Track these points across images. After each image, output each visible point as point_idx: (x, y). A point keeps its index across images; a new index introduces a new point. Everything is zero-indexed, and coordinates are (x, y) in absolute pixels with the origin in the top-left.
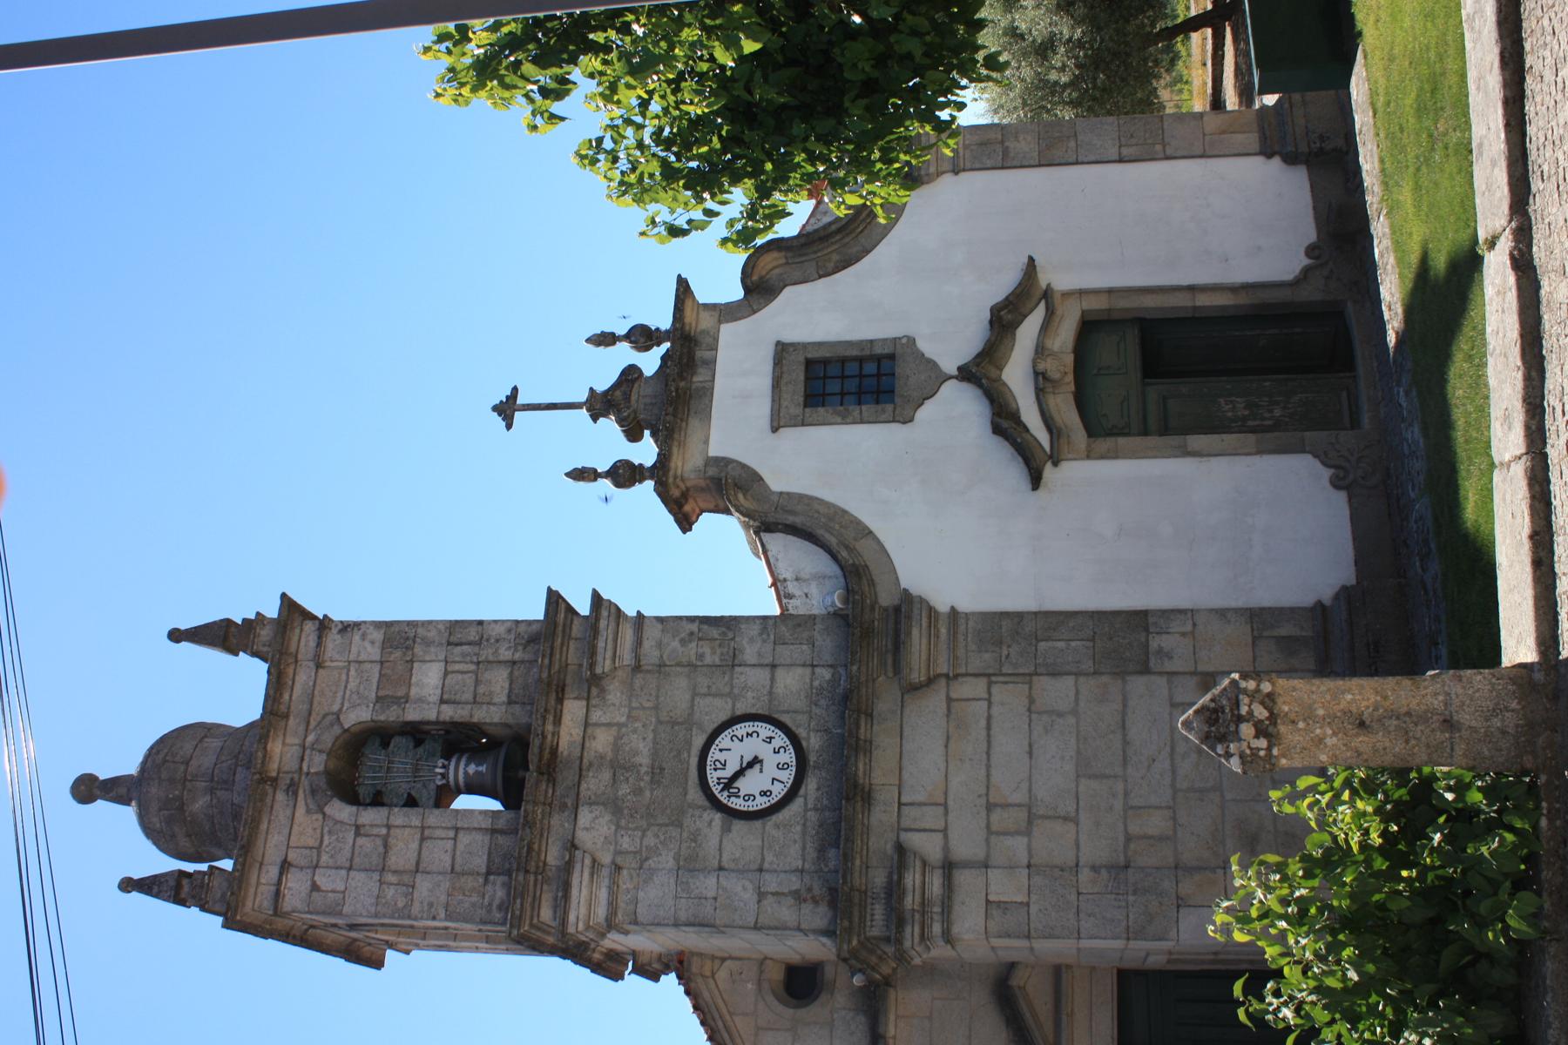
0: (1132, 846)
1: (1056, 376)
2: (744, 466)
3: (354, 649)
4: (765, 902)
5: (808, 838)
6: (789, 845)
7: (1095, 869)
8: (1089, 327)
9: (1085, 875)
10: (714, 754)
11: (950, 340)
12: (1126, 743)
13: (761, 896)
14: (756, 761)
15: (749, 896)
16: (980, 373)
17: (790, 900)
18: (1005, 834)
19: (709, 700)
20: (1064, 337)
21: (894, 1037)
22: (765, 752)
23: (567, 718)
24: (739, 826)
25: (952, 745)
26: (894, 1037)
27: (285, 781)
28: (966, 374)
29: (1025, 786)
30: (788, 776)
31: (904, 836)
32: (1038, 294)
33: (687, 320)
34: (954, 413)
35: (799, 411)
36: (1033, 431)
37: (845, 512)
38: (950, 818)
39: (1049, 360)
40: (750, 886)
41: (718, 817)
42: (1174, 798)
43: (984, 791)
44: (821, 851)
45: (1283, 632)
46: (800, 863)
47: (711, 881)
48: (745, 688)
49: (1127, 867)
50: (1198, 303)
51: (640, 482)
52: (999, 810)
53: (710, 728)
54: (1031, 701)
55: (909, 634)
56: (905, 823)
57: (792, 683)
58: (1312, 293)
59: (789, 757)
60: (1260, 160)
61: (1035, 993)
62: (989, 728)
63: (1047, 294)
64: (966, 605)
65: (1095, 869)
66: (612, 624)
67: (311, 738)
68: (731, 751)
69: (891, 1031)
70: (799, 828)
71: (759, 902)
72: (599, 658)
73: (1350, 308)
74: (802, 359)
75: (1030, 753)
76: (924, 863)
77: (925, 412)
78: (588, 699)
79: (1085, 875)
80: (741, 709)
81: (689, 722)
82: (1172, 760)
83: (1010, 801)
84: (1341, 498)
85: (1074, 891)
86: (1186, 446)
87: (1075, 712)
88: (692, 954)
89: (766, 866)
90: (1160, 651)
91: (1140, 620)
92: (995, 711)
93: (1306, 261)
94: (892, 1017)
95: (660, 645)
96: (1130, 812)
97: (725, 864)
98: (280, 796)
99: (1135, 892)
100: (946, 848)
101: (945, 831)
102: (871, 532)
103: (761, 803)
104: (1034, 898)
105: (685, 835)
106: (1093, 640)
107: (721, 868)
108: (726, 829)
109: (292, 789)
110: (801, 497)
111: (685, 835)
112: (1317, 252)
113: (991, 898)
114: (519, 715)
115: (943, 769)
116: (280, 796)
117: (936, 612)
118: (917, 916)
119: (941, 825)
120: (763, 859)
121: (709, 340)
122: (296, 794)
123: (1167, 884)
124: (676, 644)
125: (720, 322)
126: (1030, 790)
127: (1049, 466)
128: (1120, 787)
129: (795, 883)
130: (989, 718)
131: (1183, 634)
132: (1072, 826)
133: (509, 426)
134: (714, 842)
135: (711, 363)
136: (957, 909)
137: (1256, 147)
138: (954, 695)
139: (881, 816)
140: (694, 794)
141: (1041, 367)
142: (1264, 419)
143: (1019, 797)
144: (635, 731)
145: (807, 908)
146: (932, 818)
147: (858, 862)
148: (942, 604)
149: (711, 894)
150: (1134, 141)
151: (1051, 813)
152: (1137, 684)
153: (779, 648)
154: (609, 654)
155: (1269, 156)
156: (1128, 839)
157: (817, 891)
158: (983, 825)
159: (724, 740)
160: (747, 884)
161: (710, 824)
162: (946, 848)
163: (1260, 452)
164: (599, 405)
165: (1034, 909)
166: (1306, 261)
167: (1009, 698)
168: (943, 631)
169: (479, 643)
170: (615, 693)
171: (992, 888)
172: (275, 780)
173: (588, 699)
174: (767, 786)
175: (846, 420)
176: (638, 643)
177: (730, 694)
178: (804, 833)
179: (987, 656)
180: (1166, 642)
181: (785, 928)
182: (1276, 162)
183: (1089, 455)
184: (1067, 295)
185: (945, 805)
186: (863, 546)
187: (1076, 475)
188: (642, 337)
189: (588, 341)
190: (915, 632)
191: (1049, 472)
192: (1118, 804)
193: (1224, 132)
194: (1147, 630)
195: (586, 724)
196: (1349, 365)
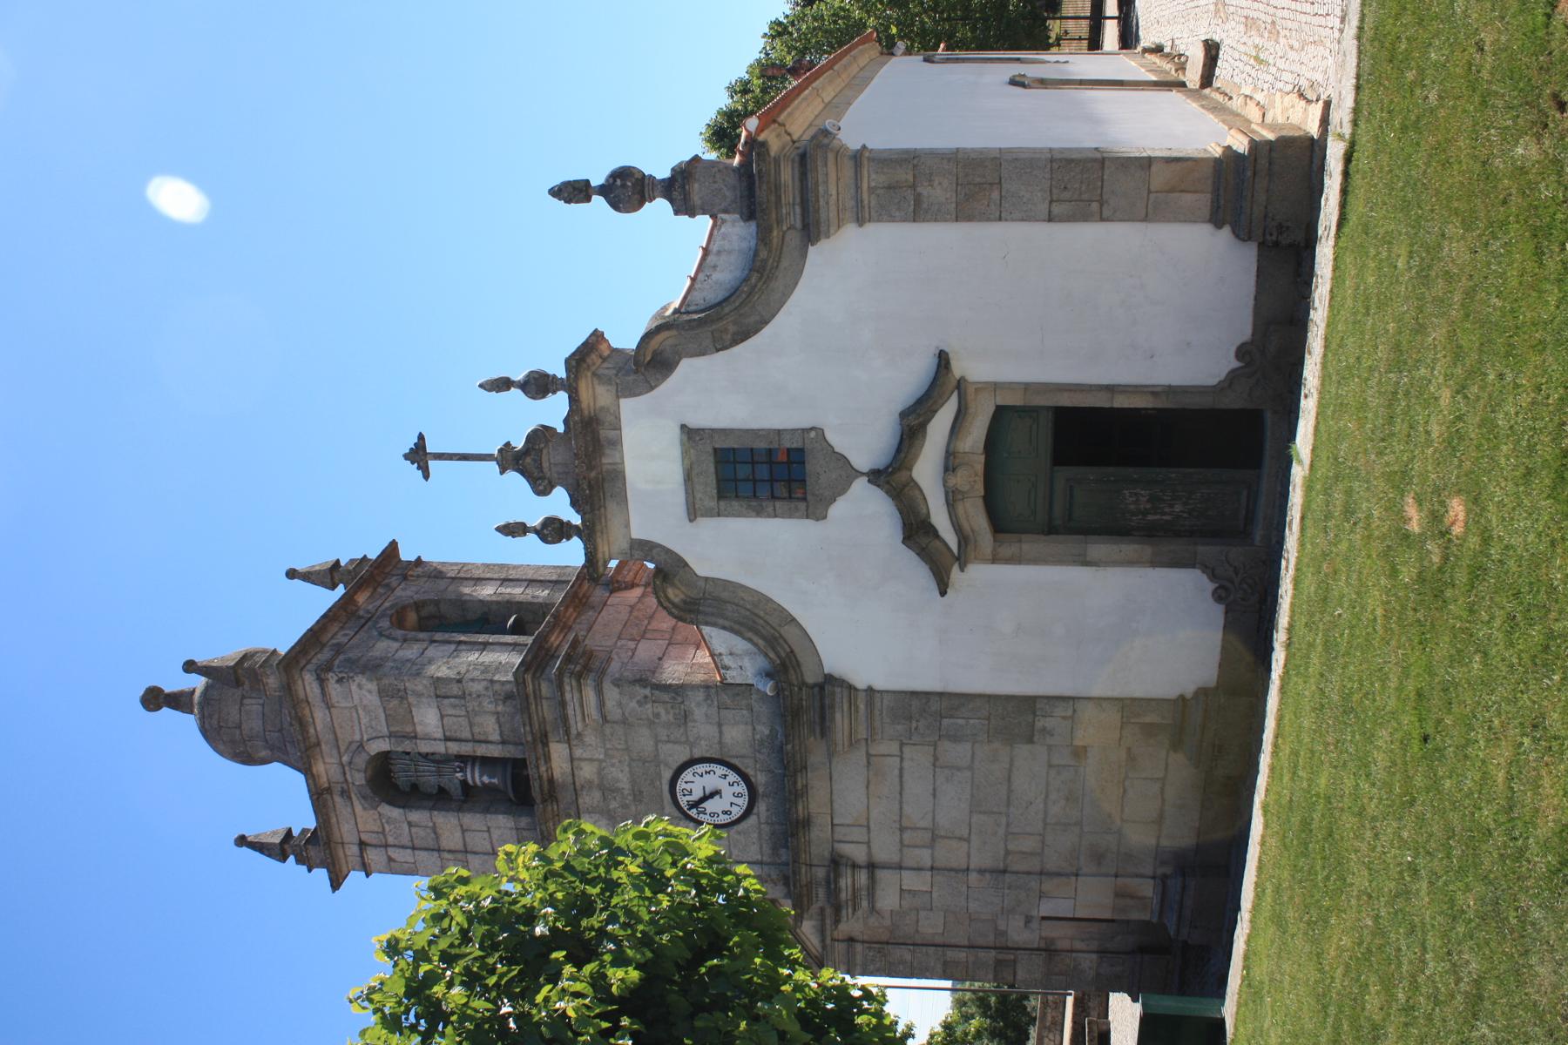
1: (966, 488)
2: (668, 551)
3: (356, 697)
7: (981, 871)
9: (973, 876)
10: (680, 785)
11: (863, 440)
12: (1010, 791)
14: (716, 793)
16: (892, 477)
19: (670, 746)
22: (723, 785)
23: (554, 756)
25: (872, 787)
27: (337, 789)
28: (876, 476)
29: (930, 817)
30: (743, 802)
31: (837, 845)
33: (584, 405)
34: (864, 512)
35: (713, 504)
37: (769, 600)
39: (960, 473)
44: (775, 849)
45: (1148, 719)
48: (699, 738)
49: (1004, 871)
50: (1116, 405)
51: (554, 392)
53: (675, 766)
54: (936, 759)
55: (833, 719)
57: (737, 735)
58: (1232, 401)
59: (742, 788)
60: (1207, 229)
62: (901, 776)
63: (961, 385)
64: (879, 684)
66: (576, 695)
67: (345, 759)
68: (695, 783)
72: (572, 722)
73: (1269, 417)
74: (710, 450)
75: (934, 795)
76: (855, 866)
77: (838, 509)
78: (568, 742)
79: (973, 876)
80: (697, 754)
81: (657, 761)
82: (1045, 804)
87: (970, 768)
90: (1044, 729)
91: (1028, 705)
92: (906, 764)
93: (1235, 364)
95: (620, 704)
98: (338, 799)
100: (869, 853)
101: (868, 843)
102: (794, 619)
106: (988, 719)
109: (345, 793)
110: (726, 584)
114: (510, 752)
116: (338, 799)
117: (856, 689)
121: (610, 418)
122: (350, 798)
124: (633, 704)
125: (618, 397)
127: (956, 568)
128: (1004, 820)
130: (901, 769)
131: (1064, 718)
132: (965, 845)
133: (426, 476)
135: (617, 443)
136: (879, 893)
137: (1206, 212)
138: (872, 752)
139: (819, 835)
141: (952, 481)
142: (1165, 514)
143: (926, 823)
144: (613, 765)
146: (858, 834)
148: (860, 680)
150: (1066, 195)
152: (1023, 750)
153: (724, 712)
154: (579, 718)
155: (1218, 225)
156: (1007, 853)
157: (774, 877)
159: (687, 775)
162: (869, 853)
163: (1154, 563)
164: (509, 459)
166: (1235, 364)
167: (918, 757)
168: (862, 707)
169: (463, 697)
170: (590, 738)
172: (329, 790)
173: (568, 742)
174: (727, 808)
175: (759, 513)
176: (601, 704)
177: (687, 742)
178: (760, 838)
179: (899, 727)
180: (1049, 723)
182: (1226, 233)
183: (995, 559)
185: (868, 827)
186: (789, 632)
187: (977, 576)
188: (538, 385)
189: (498, 529)
190: (838, 716)
192: (1001, 831)
193: (1172, 190)
194: (1035, 714)
195: (572, 760)
196: (1258, 465)
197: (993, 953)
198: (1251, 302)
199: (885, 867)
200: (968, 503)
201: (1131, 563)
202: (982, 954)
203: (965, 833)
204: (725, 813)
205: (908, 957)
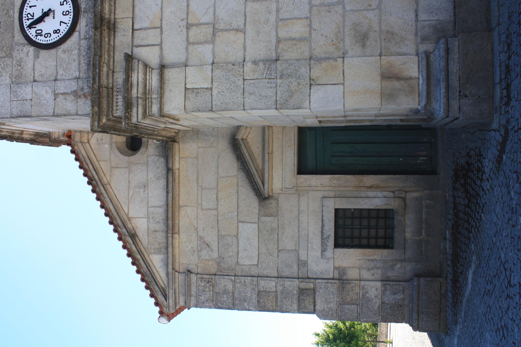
0: (281, 46)
4: (58, 100)
5: (82, 58)
6: (70, 61)
7: (255, 63)
9: (249, 66)
13: (56, 95)
15: (49, 96)
17: (71, 98)
18: (198, 43)
21: (179, 169)
24: (43, 53)
26: (179, 169)
29: (211, 11)
30: (68, 19)
31: (136, 51)
38: (164, 36)
40: (49, 90)
41: (32, 49)
42: (310, 12)
43: (185, 16)
46: (77, 73)
47: (29, 89)
49: (277, 60)
52: (195, 27)
56: (137, 42)
61: (253, 142)
65: (255, 63)
69: (177, 166)
70: (76, 52)
71: (55, 99)
76: (146, 66)
83: (201, 21)
85: (241, 79)
88: (76, 131)
89: (59, 77)
94: (177, 159)
96: (280, 23)
97: (37, 78)
99: (281, 77)
100: (161, 56)
101: (160, 45)
103: (55, 38)
104: (215, 84)
105: (14, 62)
107: (35, 81)
108: (37, 57)
111: (14, 62)
113: (188, 86)
115: (160, 5)
118: (140, 101)
119: (158, 42)
120: (57, 73)
123: (304, 71)
126: (214, 13)
129: (74, 86)
132: (241, 35)
134: (30, 65)
136: (167, 95)
140: (19, 37)
143: (207, 18)
145: (81, 101)
146: (152, 37)
147: (105, 69)
149: (29, 97)
151: (228, 27)
156: (279, 41)
158: (184, 39)
160: (48, 89)
161: (27, 54)
162: (161, 56)
165: (215, 92)
171: (189, 80)
174: (58, 27)
178: (79, 55)
181: (70, 115)
185: (161, 28)
192: (272, 18)
197: (296, 282)
199: (173, 66)
202: (288, 283)
203: (239, 22)
204: (56, 32)
205: (230, 287)
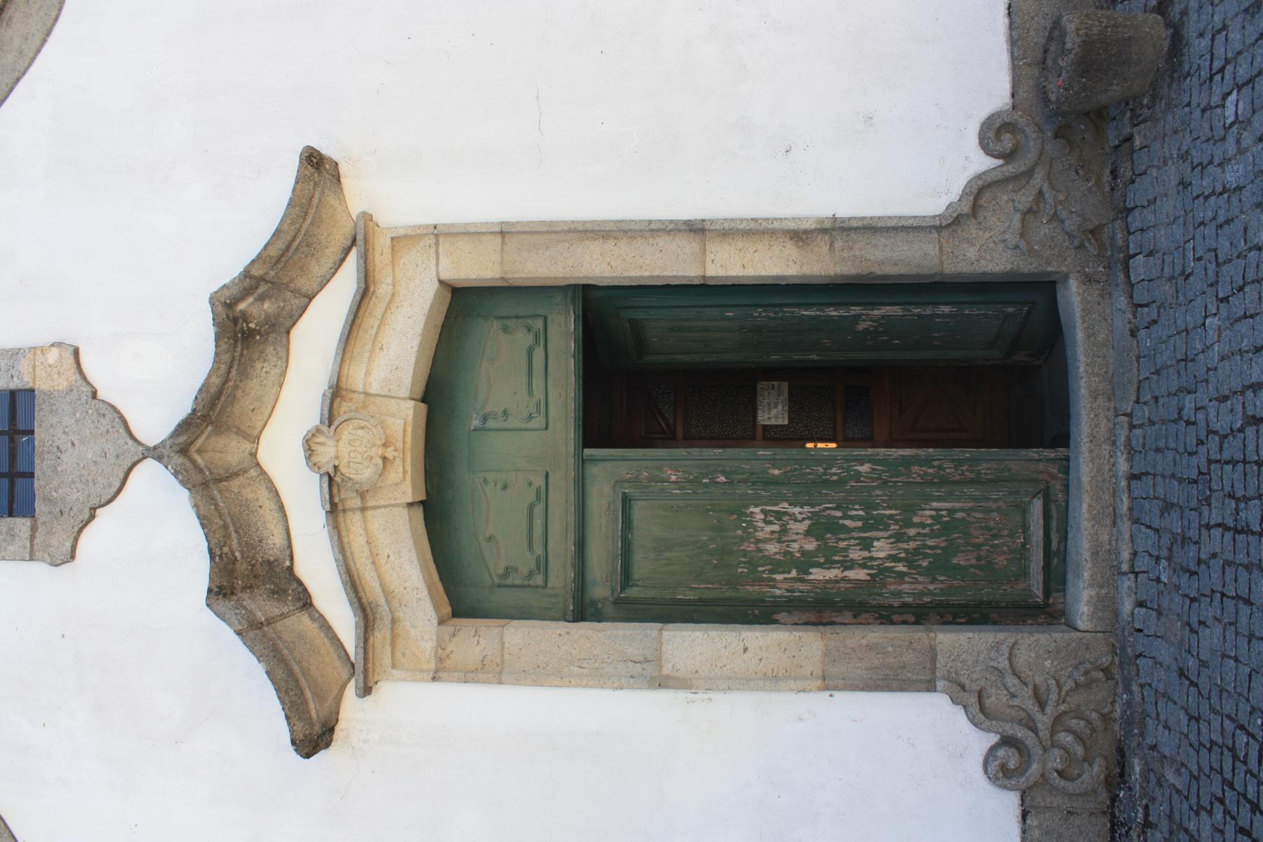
8: (464, 305)
20: (397, 357)
32: (340, 238)
36: (319, 601)
39: (347, 433)
58: (986, 254)
63: (360, 239)
73: (1073, 296)
84: (1007, 804)
86: (658, 660)
93: (982, 163)
112: (1008, 142)
142: (848, 565)
163: (829, 683)
166: (982, 163)
184: (400, 241)
191: (354, 712)
196: (1062, 439)
198: (1002, 22)
200: (377, 520)
201: (772, 680)
